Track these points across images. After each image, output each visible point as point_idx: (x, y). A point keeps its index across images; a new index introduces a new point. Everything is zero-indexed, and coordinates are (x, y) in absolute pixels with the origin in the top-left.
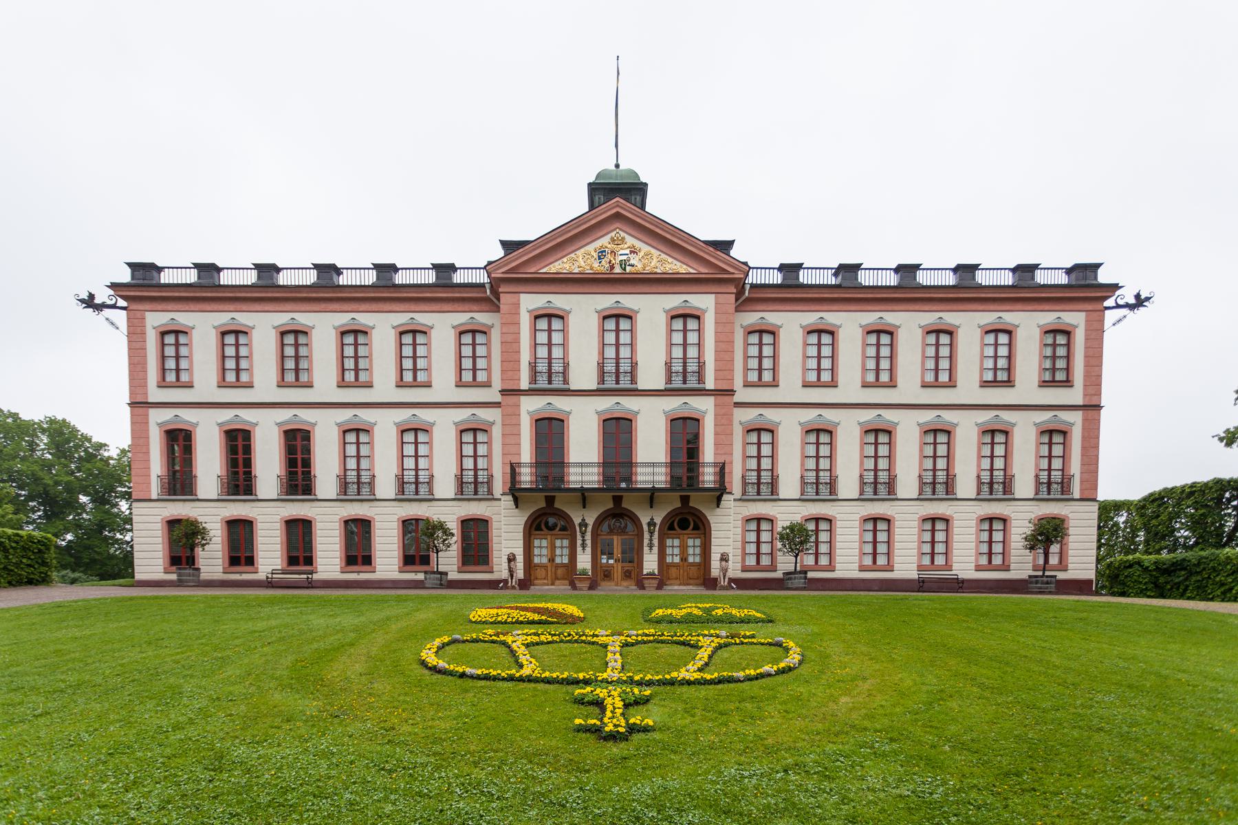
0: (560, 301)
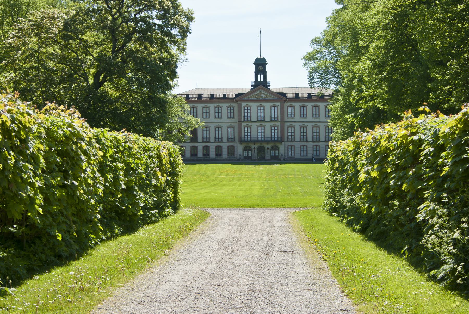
0: (250, 104)
